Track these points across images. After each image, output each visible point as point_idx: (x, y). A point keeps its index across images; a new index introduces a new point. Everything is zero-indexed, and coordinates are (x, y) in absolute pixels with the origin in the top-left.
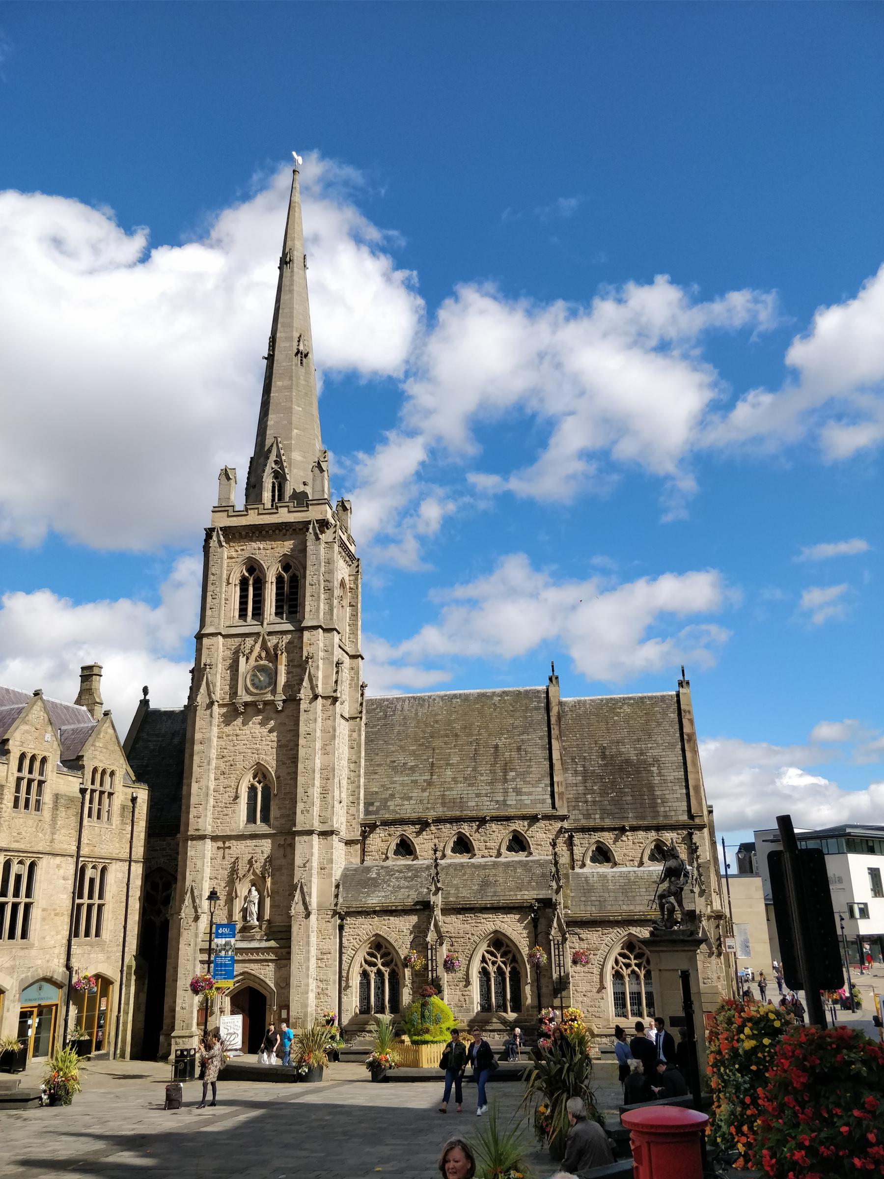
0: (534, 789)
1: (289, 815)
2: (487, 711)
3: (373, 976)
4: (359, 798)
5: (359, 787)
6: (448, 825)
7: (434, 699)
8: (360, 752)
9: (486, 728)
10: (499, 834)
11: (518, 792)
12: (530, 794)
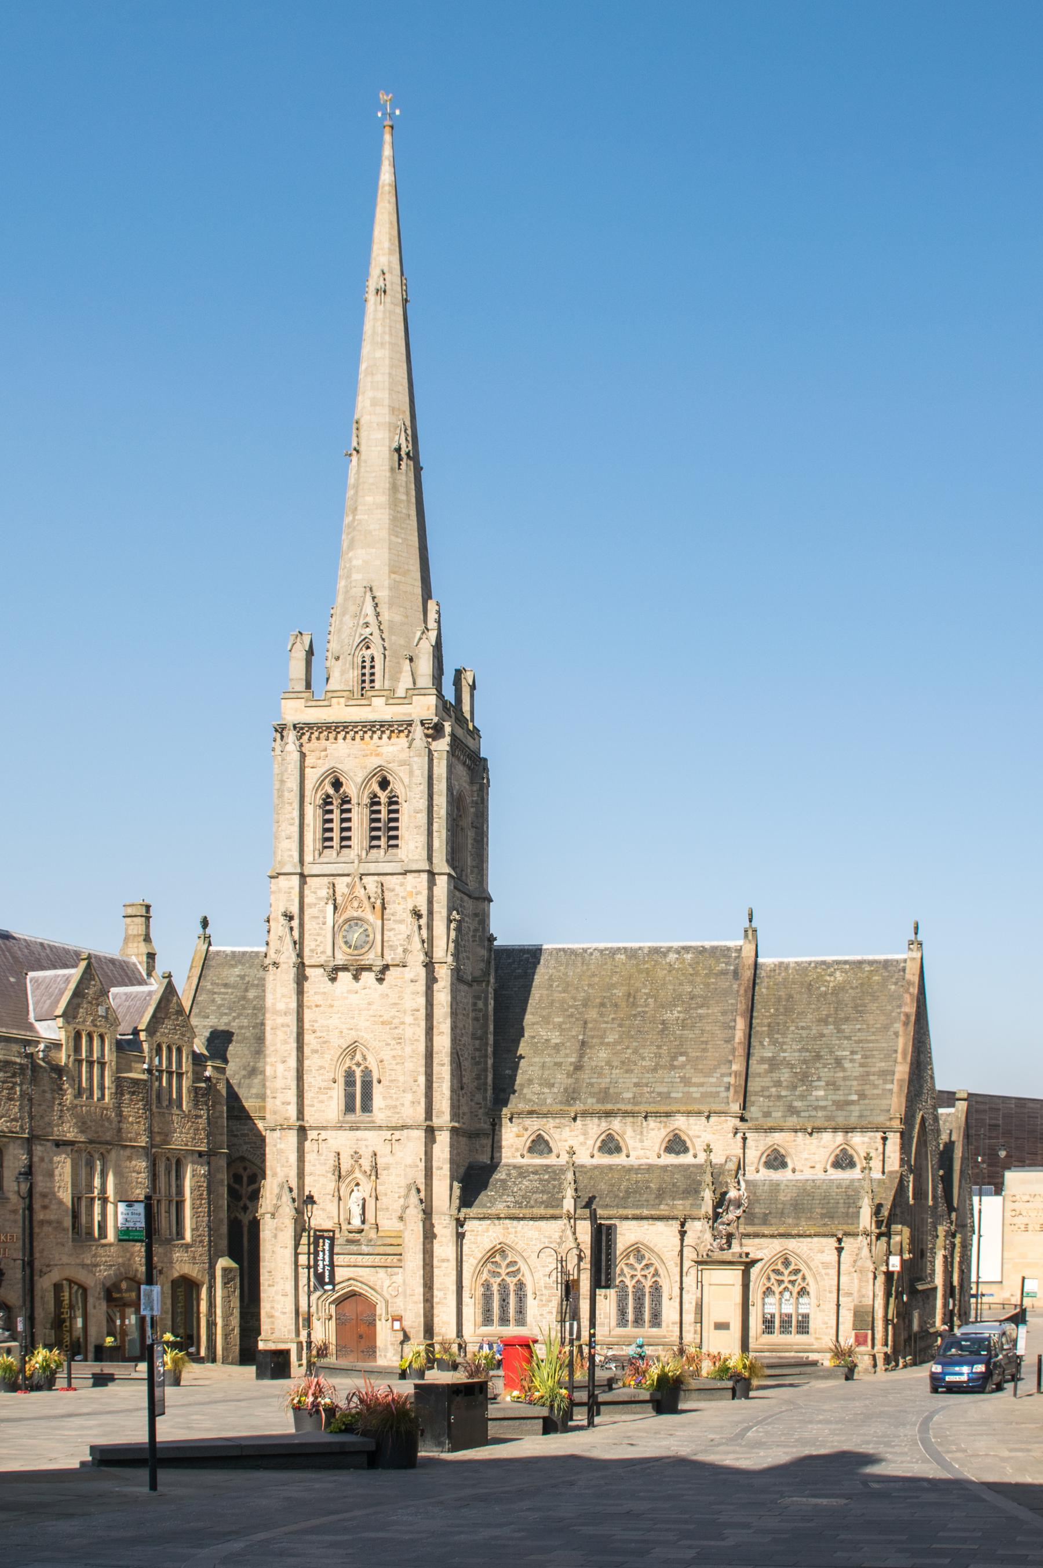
0: (706, 1080)
1: (395, 1107)
2: (661, 973)
3: (495, 1288)
4: (486, 1084)
5: (485, 1070)
6: (596, 1120)
7: (591, 954)
8: (486, 1025)
9: (656, 998)
10: (656, 1133)
11: (686, 1081)
12: (702, 1085)
